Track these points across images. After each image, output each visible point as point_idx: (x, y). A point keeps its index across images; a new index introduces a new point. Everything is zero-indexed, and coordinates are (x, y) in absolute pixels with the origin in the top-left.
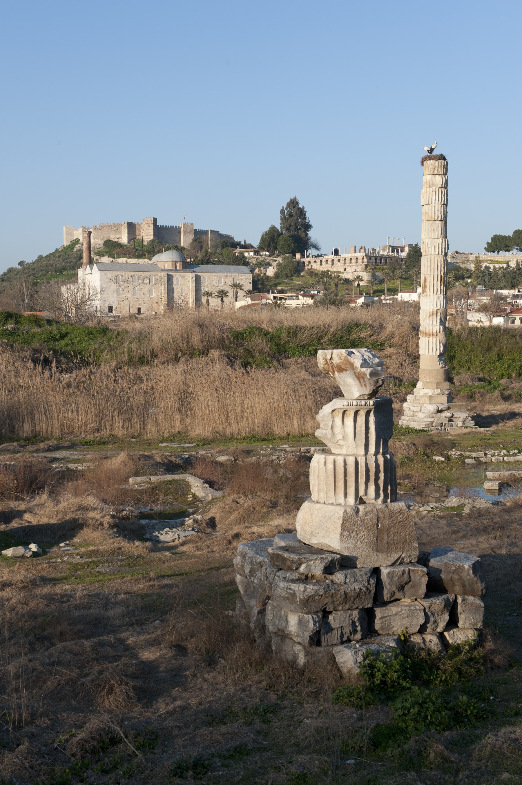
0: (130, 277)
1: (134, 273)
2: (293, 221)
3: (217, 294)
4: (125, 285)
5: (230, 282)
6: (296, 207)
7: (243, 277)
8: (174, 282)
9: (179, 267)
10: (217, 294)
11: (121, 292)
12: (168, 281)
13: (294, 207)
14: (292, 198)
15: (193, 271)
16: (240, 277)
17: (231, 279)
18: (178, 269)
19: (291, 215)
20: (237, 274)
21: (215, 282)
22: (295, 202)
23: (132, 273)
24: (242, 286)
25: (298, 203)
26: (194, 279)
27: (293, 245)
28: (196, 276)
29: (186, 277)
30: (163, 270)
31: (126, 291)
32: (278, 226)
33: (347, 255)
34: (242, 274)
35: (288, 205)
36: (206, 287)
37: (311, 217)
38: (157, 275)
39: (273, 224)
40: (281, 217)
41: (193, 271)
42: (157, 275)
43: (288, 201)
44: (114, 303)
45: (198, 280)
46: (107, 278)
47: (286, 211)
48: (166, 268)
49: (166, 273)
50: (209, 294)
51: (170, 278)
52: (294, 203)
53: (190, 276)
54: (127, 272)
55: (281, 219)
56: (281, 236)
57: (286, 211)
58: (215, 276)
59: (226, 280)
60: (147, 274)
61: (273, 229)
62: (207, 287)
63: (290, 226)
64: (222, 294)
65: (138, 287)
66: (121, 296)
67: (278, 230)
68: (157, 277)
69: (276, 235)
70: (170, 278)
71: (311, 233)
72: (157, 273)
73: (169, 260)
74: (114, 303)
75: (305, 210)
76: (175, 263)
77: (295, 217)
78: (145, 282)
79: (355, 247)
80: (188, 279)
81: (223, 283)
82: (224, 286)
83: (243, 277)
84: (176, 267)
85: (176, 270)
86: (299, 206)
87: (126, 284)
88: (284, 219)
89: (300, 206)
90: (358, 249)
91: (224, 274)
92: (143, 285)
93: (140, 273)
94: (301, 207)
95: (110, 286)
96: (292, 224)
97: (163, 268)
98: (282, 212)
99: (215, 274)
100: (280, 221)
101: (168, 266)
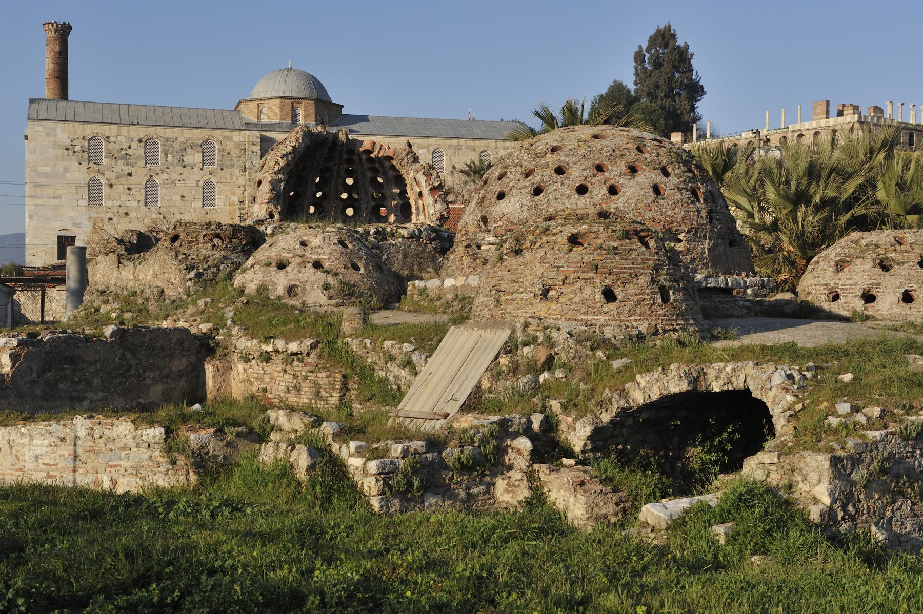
0: (135, 145)
1: (151, 131)
2: (661, 77)
4: (117, 169)
6: (671, 43)
9: (306, 117)
11: (105, 191)
14: (662, 27)
19: (657, 64)
20: (492, 144)
22: (667, 34)
23: (142, 132)
25: (673, 36)
27: (662, 121)
31: (120, 188)
32: (630, 83)
33: (806, 125)
35: (653, 41)
37: (702, 68)
38: (229, 138)
39: (619, 79)
40: (636, 68)
42: (229, 138)
43: (652, 32)
44: (79, 225)
46: (55, 145)
47: (647, 56)
48: (264, 120)
49: (257, 134)
52: (664, 37)
54: (124, 128)
56: (636, 105)
60: (197, 135)
61: (617, 90)
63: (657, 86)
65: (165, 176)
66: (106, 203)
67: (629, 91)
68: (229, 146)
71: (702, 107)
72: (227, 133)
73: (274, 94)
74: (79, 225)
75: (690, 51)
77: (667, 67)
78: (188, 159)
79: (828, 102)
84: (294, 118)
86: (677, 44)
87: (120, 166)
88: (641, 75)
89: (680, 42)
90: (833, 111)
91: (448, 142)
92: (179, 169)
93: (168, 130)
94: (682, 45)
95: (66, 170)
96: (661, 82)
97: (256, 121)
98: (639, 57)
100: (634, 78)
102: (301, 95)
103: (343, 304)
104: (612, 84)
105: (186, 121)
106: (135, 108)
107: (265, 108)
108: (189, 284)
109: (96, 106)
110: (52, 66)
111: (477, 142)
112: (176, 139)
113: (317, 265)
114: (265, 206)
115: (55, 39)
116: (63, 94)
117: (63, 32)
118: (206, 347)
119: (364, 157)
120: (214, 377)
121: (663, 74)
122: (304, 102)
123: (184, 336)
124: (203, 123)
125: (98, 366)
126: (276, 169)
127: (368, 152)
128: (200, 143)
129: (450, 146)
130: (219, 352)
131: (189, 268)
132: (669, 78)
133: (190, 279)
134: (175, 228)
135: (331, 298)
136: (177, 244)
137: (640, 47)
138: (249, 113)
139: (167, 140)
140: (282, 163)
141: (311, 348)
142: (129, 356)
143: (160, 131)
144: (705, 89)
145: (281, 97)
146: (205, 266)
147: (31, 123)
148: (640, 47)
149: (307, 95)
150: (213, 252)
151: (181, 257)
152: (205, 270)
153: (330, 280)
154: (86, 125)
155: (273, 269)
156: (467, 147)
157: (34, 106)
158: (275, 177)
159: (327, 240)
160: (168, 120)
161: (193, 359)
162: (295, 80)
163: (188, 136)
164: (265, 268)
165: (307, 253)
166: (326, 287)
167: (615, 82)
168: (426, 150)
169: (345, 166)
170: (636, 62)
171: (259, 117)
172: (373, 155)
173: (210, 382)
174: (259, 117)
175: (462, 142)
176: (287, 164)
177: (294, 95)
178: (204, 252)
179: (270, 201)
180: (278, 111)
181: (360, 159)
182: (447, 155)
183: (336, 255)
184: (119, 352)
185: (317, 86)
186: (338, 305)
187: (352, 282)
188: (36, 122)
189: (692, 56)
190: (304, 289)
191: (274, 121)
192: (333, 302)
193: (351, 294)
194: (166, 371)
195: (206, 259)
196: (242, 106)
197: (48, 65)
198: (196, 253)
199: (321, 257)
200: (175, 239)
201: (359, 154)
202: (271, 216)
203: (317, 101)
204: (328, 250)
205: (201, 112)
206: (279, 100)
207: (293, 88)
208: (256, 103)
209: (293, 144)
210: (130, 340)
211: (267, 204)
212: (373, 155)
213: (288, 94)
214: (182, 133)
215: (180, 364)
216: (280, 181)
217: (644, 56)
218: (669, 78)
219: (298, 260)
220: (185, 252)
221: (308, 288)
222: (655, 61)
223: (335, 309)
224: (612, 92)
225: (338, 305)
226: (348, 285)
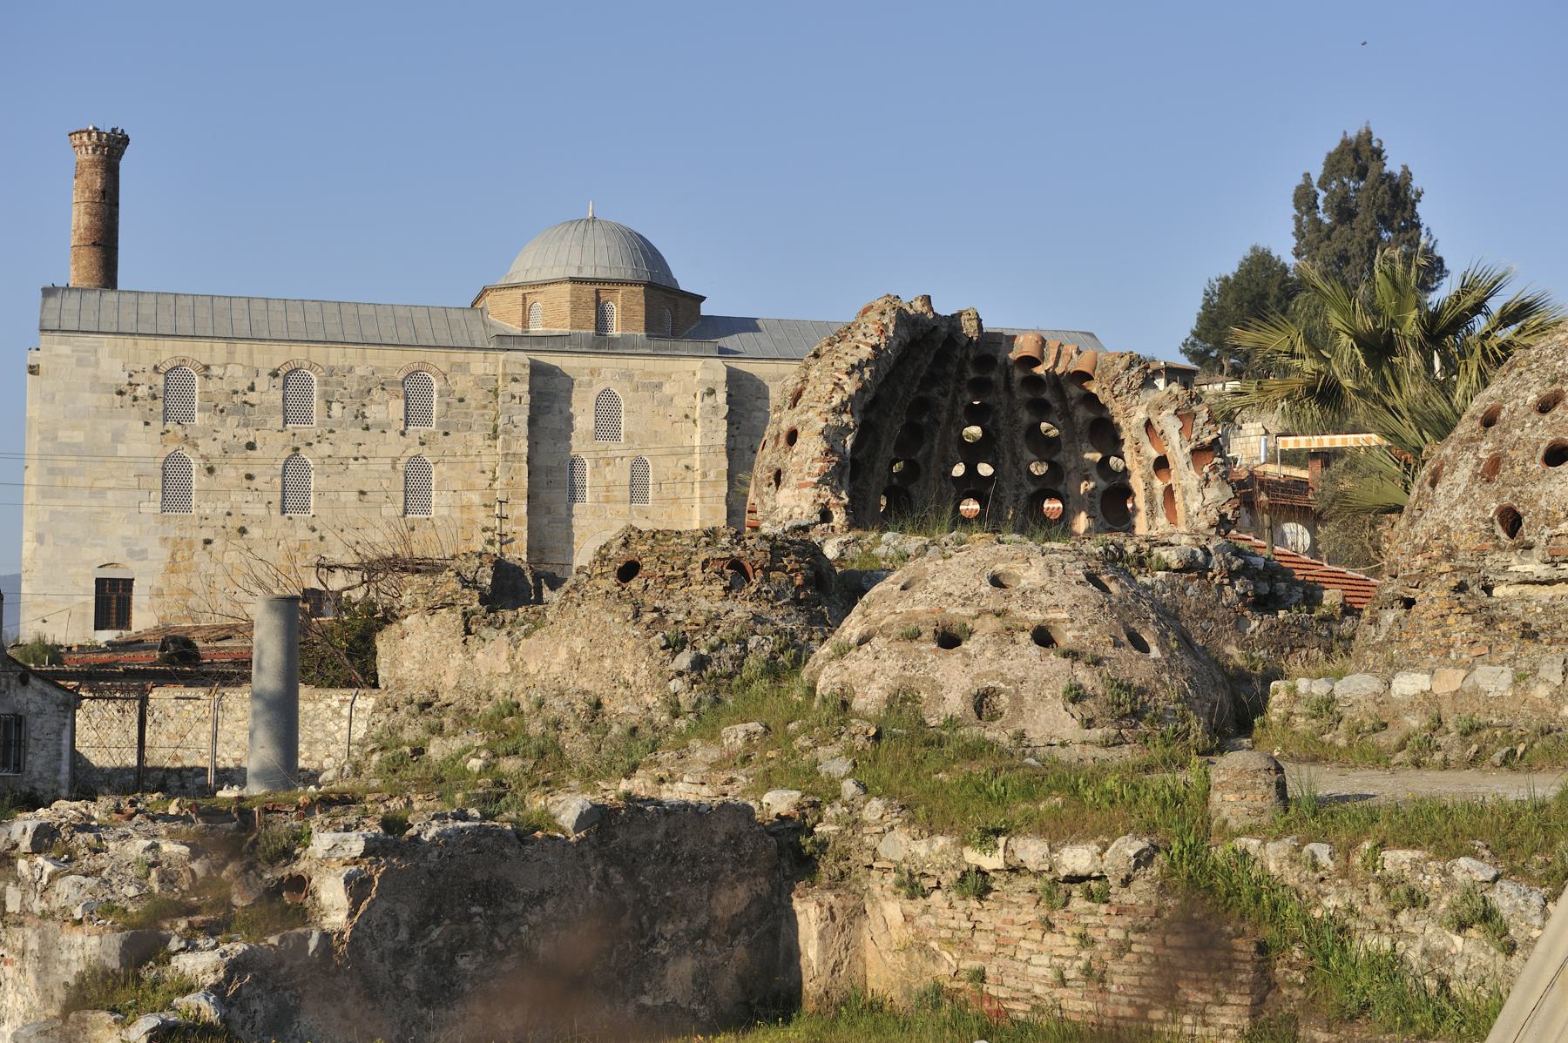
0: (262, 383)
1: (298, 353)
4: (225, 435)
6: (1373, 168)
9: (625, 322)
11: (198, 479)
13: (1362, 173)
14: (1352, 134)
15: (723, 352)
18: (615, 331)
19: (1344, 212)
23: (279, 356)
25: (1378, 154)
26: (721, 397)
28: (736, 381)
29: (668, 389)
31: (230, 474)
32: (1284, 249)
35: (1334, 165)
38: (463, 368)
39: (1263, 244)
40: (1298, 220)
42: (463, 368)
43: (1333, 145)
44: (142, 555)
46: (96, 384)
47: (1322, 194)
48: (537, 329)
49: (523, 357)
51: (548, 396)
52: (1358, 156)
54: (241, 347)
55: (1299, 234)
57: (1322, 194)
60: (395, 362)
61: (1261, 263)
65: (325, 449)
66: (200, 505)
67: (1284, 269)
68: (462, 384)
69: (1274, 291)
72: (458, 356)
73: (559, 273)
74: (142, 555)
75: (1416, 184)
78: (374, 413)
80: (681, 402)
84: (601, 323)
85: (601, 342)
86: (1387, 170)
87: (231, 430)
88: (1310, 237)
89: (1393, 166)
92: (356, 433)
94: (1398, 171)
95: (117, 437)
96: (1353, 250)
97: (518, 331)
98: (1304, 198)
100: (1293, 242)
102: (615, 275)
103: (1119, 741)
104: (1249, 254)
105: (370, 333)
106: (263, 305)
107: (539, 302)
108: (676, 685)
109: (182, 302)
112: (351, 370)
113: (1043, 637)
114: (811, 493)
115: (94, 164)
116: (108, 275)
117: (112, 148)
118: (792, 854)
119: (1018, 374)
120: (821, 936)
121: (1358, 233)
122: (622, 290)
123: (743, 826)
124: (406, 335)
125: (549, 906)
126: (836, 401)
127: (1029, 362)
128: (400, 378)
130: (827, 867)
131: (675, 645)
132: (1370, 242)
133: (680, 674)
134: (625, 545)
135: (1089, 723)
136: (635, 584)
137: (1307, 176)
138: (504, 314)
139: (331, 371)
140: (851, 386)
141: (1137, 865)
142: (618, 879)
143: (317, 352)
144: (1447, 265)
145: (573, 280)
146: (714, 640)
147: (46, 337)
148: (1307, 176)
149: (629, 276)
150: (728, 605)
151: (648, 617)
152: (713, 649)
153: (1084, 675)
154: (161, 342)
155: (928, 647)
157: (53, 302)
158: (833, 422)
159: (1059, 573)
160: (333, 331)
161: (763, 885)
162: (603, 242)
163: (375, 363)
164: (904, 646)
165: (1013, 606)
166: (1076, 695)
167: (1254, 249)
169: (968, 396)
170: (1297, 207)
171: (525, 322)
172: (1040, 370)
173: (811, 950)
174: (525, 322)
176: (862, 391)
177: (601, 275)
178: (704, 604)
179: (823, 481)
180: (566, 308)
181: (1008, 379)
183: (1089, 611)
184: (596, 870)
185: (649, 255)
186: (1106, 744)
187: (1137, 683)
188: (57, 337)
189: (1419, 195)
190: (1017, 699)
191: (557, 331)
192: (1096, 733)
193: (1137, 715)
194: (702, 919)
195: (713, 620)
196: (488, 300)
197: (77, 218)
198: (685, 606)
199: (1052, 615)
200: (628, 571)
201: (1007, 368)
202: (826, 516)
203: (650, 287)
204: (1066, 599)
205: (401, 312)
206: (568, 287)
207: (601, 260)
208: (521, 291)
209: (874, 341)
210: (621, 836)
211: (816, 486)
212: (1040, 370)
213: (587, 273)
214: (364, 358)
215: (733, 899)
216: (845, 429)
217: (1316, 196)
218: (1370, 242)
219: (992, 623)
220: (658, 604)
221: (1028, 698)
222: (1339, 206)
223: (1102, 753)
224: (1249, 272)
225: (1106, 744)
226: (1128, 688)
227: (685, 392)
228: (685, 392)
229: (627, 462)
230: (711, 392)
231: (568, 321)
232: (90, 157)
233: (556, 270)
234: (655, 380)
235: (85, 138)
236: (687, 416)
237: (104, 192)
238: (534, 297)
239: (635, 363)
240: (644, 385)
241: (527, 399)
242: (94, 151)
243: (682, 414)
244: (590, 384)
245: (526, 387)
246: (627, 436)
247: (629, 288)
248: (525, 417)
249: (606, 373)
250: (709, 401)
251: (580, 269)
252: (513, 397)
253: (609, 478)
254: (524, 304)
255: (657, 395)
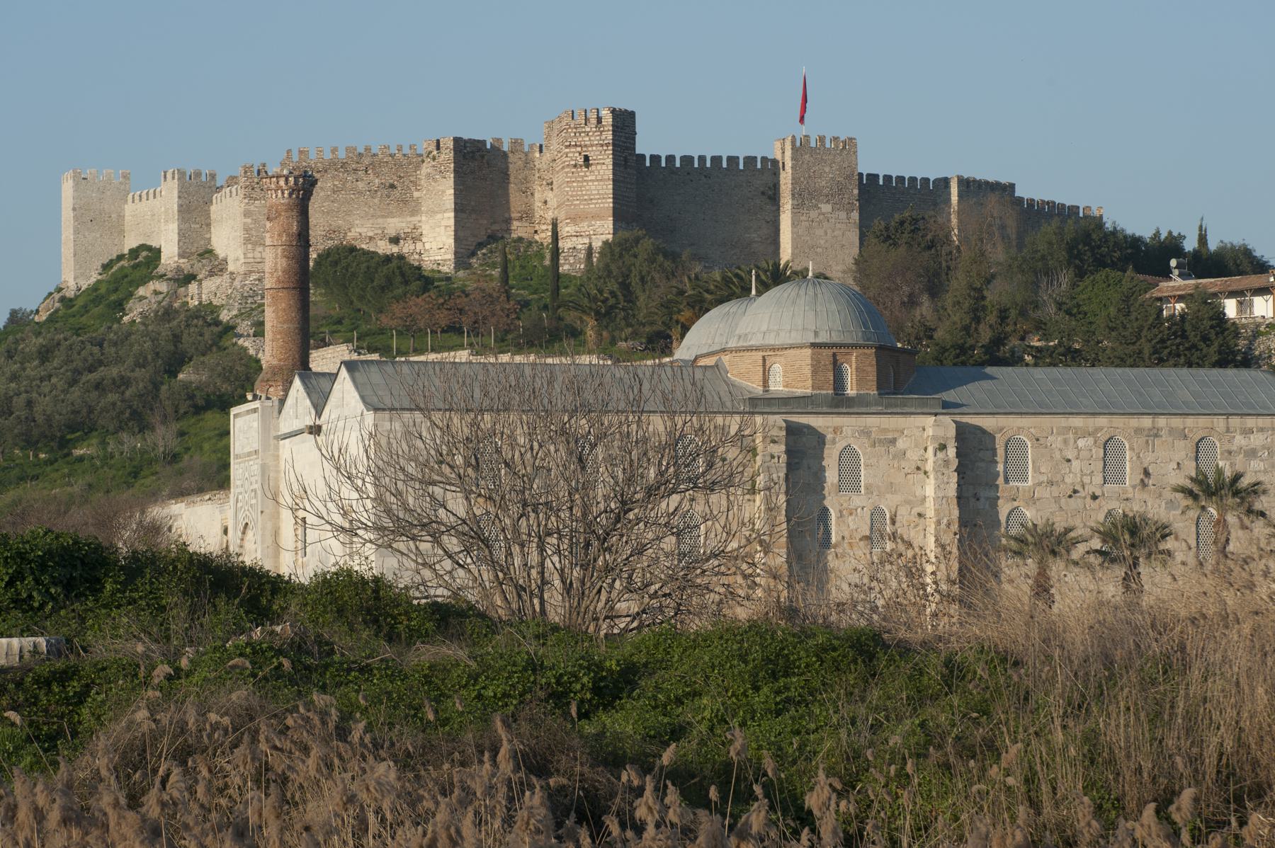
3: (1096, 544)
5: (1173, 464)
7: (1257, 440)
8: (831, 476)
9: (860, 382)
10: (1096, 544)
12: (790, 466)
15: (946, 405)
16: (1239, 440)
17: (1182, 451)
18: (851, 391)
20: (1220, 423)
21: (1083, 468)
24: (1256, 489)
26: (952, 452)
29: (901, 444)
30: (762, 403)
34: (1250, 422)
36: (1027, 499)
41: (946, 405)
45: (975, 462)
48: (778, 385)
49: (779, 420)
50: (1052, 543)
53: (924, 435)
58: (1081, 433)
59: (1148, 458)
62: (1032, 500)
64: (1131, 540)
70: (803, 450)
73: (796, 338)
76: (829, 356)
80: (914, 455)
81: (1131, 475)
82: (1139, 495)
83: (1257, 440)
84: (839, 383)
85: (839, 402)
91: (1134, 422)
97: (758, 390)
99: (1077, 422)
101: (790, 376)
110: (282, 263)
111: (1190, 421)
115: (289, 208)
129: (1138, 431)
145: (813, 345)
156: (1171, 431)
162: (834, 307)
168: (1091, 440)
175: (1162, 422)
177: (836, 338)
180: (807, 371)
182: (1132, 449)
191: (799, 392)
206: (808, 352)
208: (761, 354)
227: (916, 446)
228: (916, 446)
229: (867, 512)
230: (943, 447)
231: (810, 382)
232: (286, 201)
233: (794, 334)
234: (890, 436)
235: (282, 182)
236: (918, 468)
237: (299, 235)
238: (773, 359)
239: (872, 421)
240: (880, 441)
241: (784, 457)
242: (290, 195)
243: (913, 467)
244: (834, 441)
245: (783, 448)
246: (867, 488)
247: (861, 351)
248: (782, 475)
249: (847, 431)
250: (940, 455)
251: (816, 334)
252: (773, 457)
253: (852, 526)
254: (764, 365)
255: (892, 449)
